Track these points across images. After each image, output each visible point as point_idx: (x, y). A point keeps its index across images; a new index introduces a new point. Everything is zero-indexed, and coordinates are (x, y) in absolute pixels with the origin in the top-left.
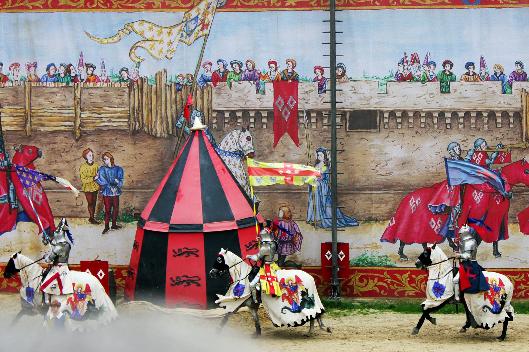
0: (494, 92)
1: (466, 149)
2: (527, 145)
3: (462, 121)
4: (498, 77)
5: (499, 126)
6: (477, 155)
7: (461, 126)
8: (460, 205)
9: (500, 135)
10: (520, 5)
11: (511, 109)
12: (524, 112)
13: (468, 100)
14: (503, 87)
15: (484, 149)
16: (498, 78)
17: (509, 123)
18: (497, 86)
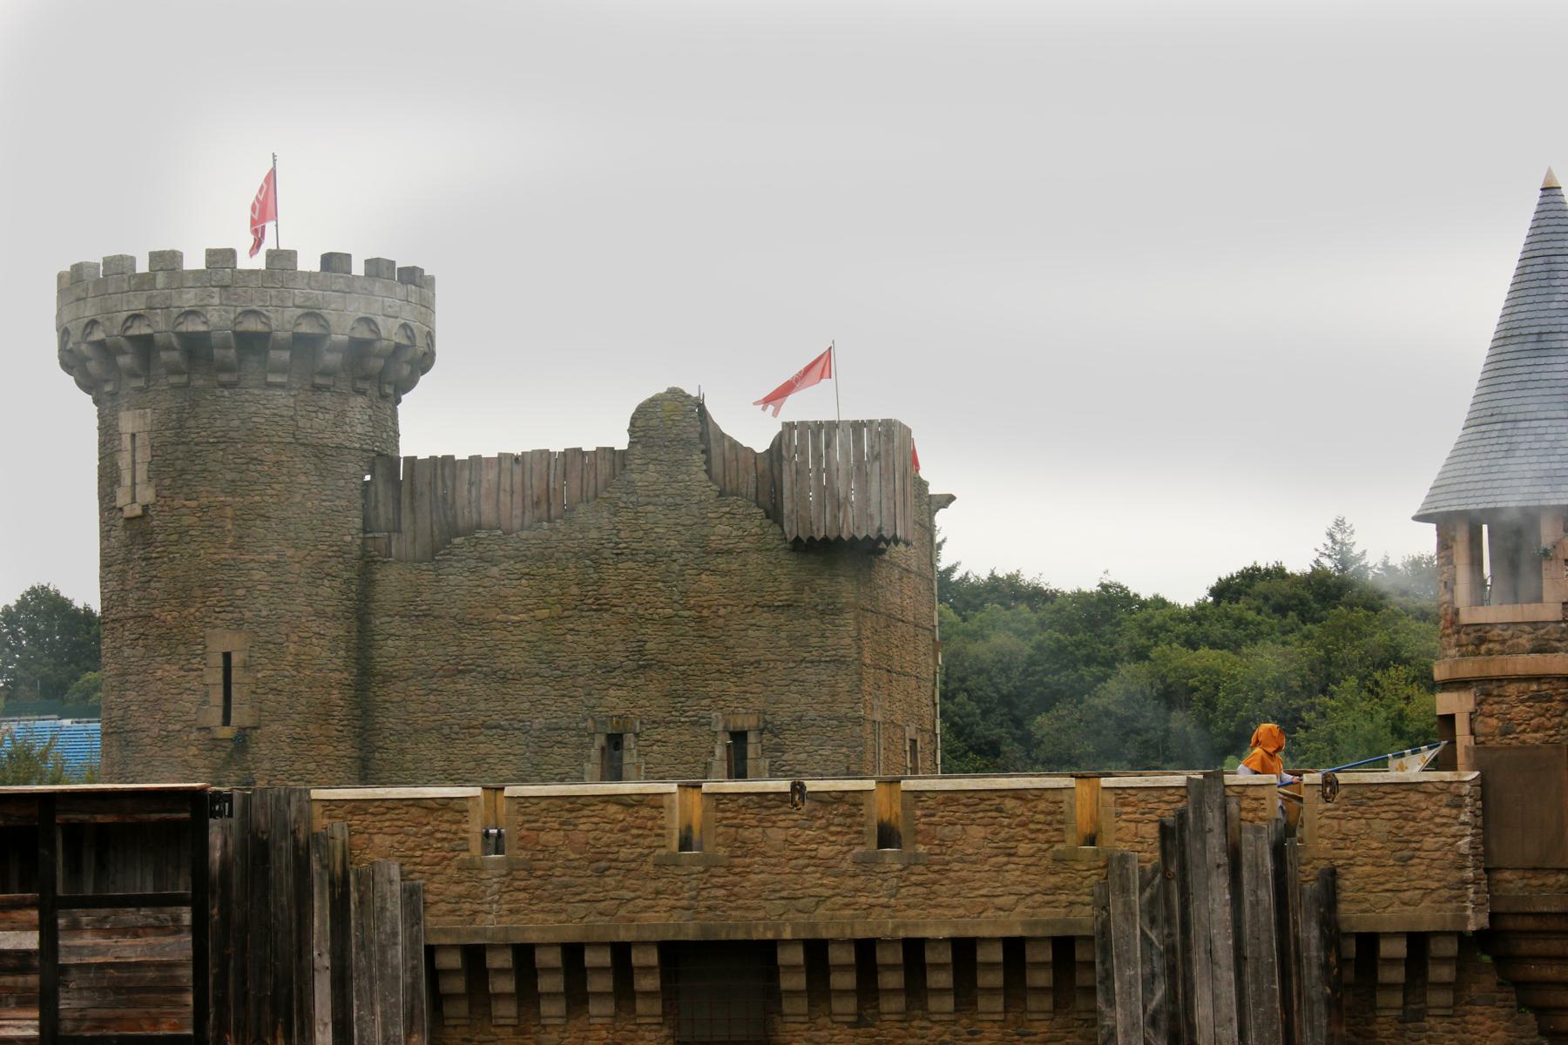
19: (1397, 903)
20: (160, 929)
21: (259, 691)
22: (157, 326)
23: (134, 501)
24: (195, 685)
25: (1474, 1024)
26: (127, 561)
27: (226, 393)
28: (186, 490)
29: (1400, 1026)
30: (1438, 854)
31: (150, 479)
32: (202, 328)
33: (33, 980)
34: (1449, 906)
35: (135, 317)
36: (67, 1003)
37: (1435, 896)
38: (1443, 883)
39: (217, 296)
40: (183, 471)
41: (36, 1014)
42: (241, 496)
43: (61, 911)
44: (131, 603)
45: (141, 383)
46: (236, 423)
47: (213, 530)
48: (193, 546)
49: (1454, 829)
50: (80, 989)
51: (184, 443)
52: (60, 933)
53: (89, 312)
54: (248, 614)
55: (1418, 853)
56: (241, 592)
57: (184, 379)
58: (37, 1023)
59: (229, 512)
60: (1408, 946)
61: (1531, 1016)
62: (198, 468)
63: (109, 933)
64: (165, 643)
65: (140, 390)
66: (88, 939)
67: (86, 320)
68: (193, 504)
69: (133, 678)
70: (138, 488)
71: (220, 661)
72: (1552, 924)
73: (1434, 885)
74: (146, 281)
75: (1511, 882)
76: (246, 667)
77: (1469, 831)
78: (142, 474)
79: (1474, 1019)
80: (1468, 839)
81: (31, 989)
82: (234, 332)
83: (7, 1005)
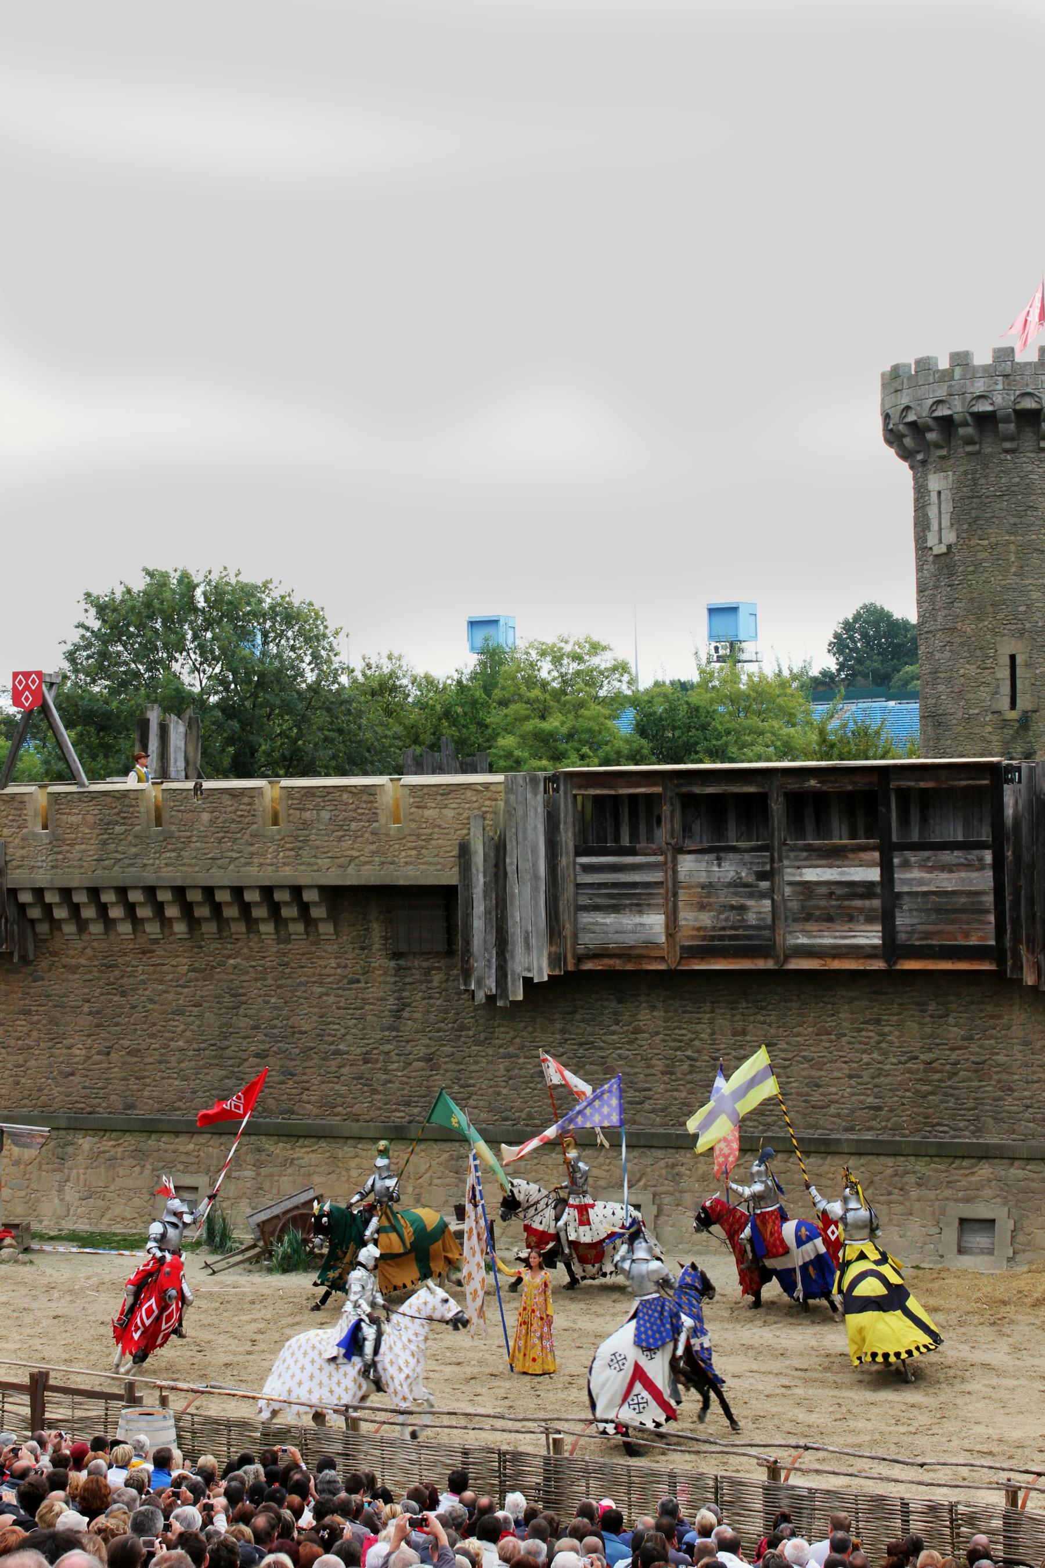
20: (969, 866)
21: (1038, 683)
22: (956, 408)
23: (940, 542)
24: (989, 679)
26: (936, 587)
27: (1009, 457)
28: (979, 532)
31: (952, 525)
32: (990, 408)
33: (876, 903)
35: (939, 402)
36: (902, 920)
39: (1000, 383)
40: (977, 518)
41: (880, 928)
42: (1022, 535)
43: (896, 853)
44: (940, 619)
45: (944, 452)
46: (1017, 480)
47: (1001, 562)
48: (986, 574)
50: (911, 910)
51: (977, 497)
52: (896, 869)
53: (905, 400)
54: (1028, 625)
56: (1022, 609)
57: (977, 448)
58: (880, 934)
59: (1012, 547)
62: (988, 515)
63: (931, 869)
64: (966, 648)
65: (943, 458)
66: (915, 874)
67: (903, 407)
68: (986, 542)
69: (942, 675)
70: (943, 532)
71: (1007, 661)
74: (946, 376)
76: (1027, 665)
78: (946, 521)
81: (875, 910)
82: (1015, 410)
83: (858, 921)
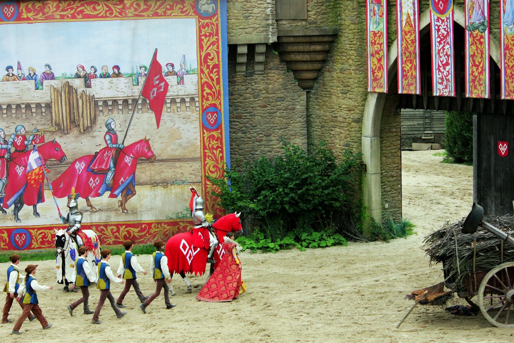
0: (29, 89)
1: (8, 133)
2: (57, 129)
3: (5, 111)
4: (32, 76)
5: (34, 115)
6: (18, 138)
7: (5, 116)
8: (6, 177)
9: (35, 122)
10: (46, 21)
11: (43, 101)
12: (53, 104)
13: (9, 95)
14: (36, 85)
15: (23, 133)
16: (32, 77)
17: (42, 112)
18: (31, 84)
19: (244, 33)
25: (272, 77)
29: (244, 78)
30: (259, 15)
34: (262, 34)
37: (258, 30)
38: (261, 25)
49: (265, 5)
55: (251, 15)
60: (248, 49)
61: (292, 73)
72: (300, 40)
73: (258, 26)
75: (285, 25)
77: (270, 6)
79: (271, 75)
80: (270, 9)
